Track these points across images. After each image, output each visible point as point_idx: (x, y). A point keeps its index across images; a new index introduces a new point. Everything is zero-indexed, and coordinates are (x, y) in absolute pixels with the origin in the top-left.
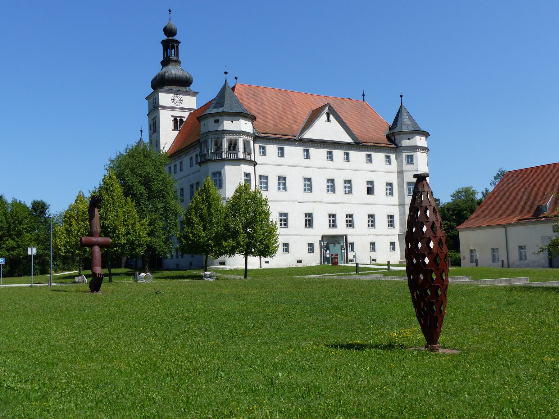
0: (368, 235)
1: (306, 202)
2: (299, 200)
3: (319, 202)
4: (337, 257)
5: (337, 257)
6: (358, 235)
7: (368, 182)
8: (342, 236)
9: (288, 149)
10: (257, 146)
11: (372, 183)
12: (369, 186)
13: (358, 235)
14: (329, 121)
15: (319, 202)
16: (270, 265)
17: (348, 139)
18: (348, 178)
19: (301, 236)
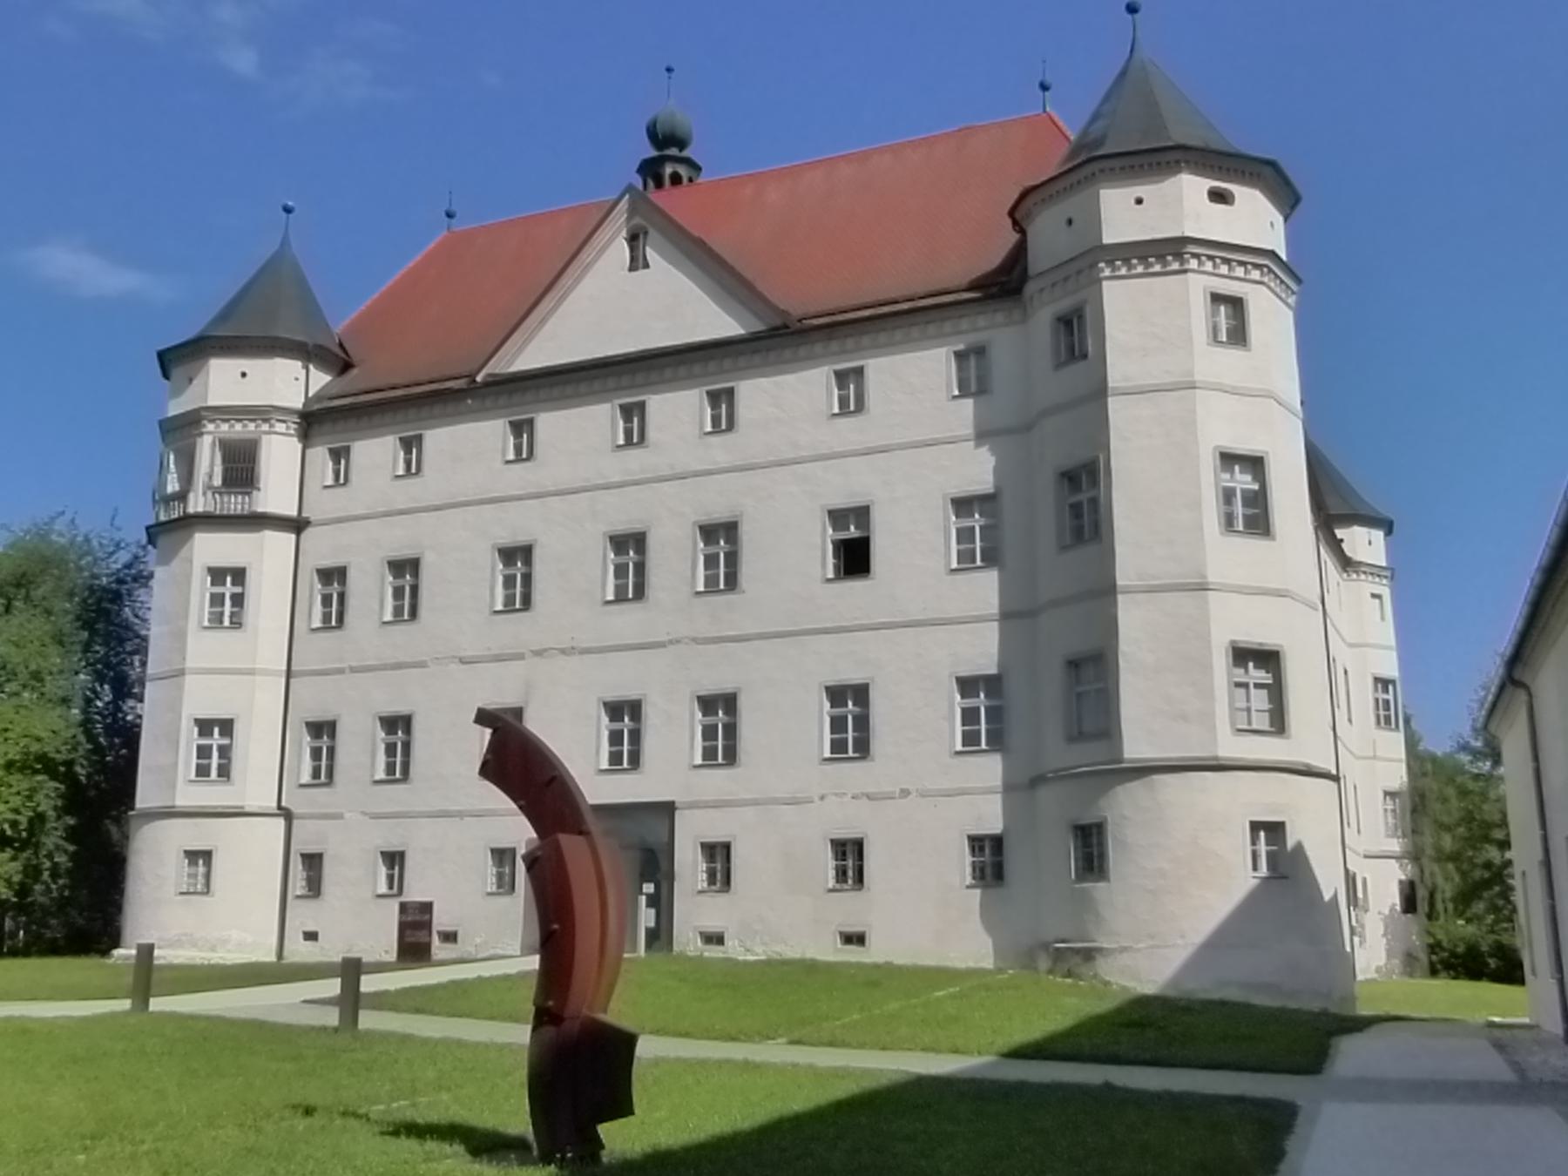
0: (905, 793)
1: (498, 659)
2: (468, 653)
3: (563, 651)
4: (427, 917)
5: (427, 917)
6: (755, 803)
7: (838, 517)
8: (667, 810)
9: (441, 439)
10: (320, 455)
11: (862, 514)
12: (853, 532)
13: (755, 803)
14: (637, 262)
15: (563, 651)
16: (322, 948)
17: (719, 323)
18: (719, 514)
19: (461, 814)
